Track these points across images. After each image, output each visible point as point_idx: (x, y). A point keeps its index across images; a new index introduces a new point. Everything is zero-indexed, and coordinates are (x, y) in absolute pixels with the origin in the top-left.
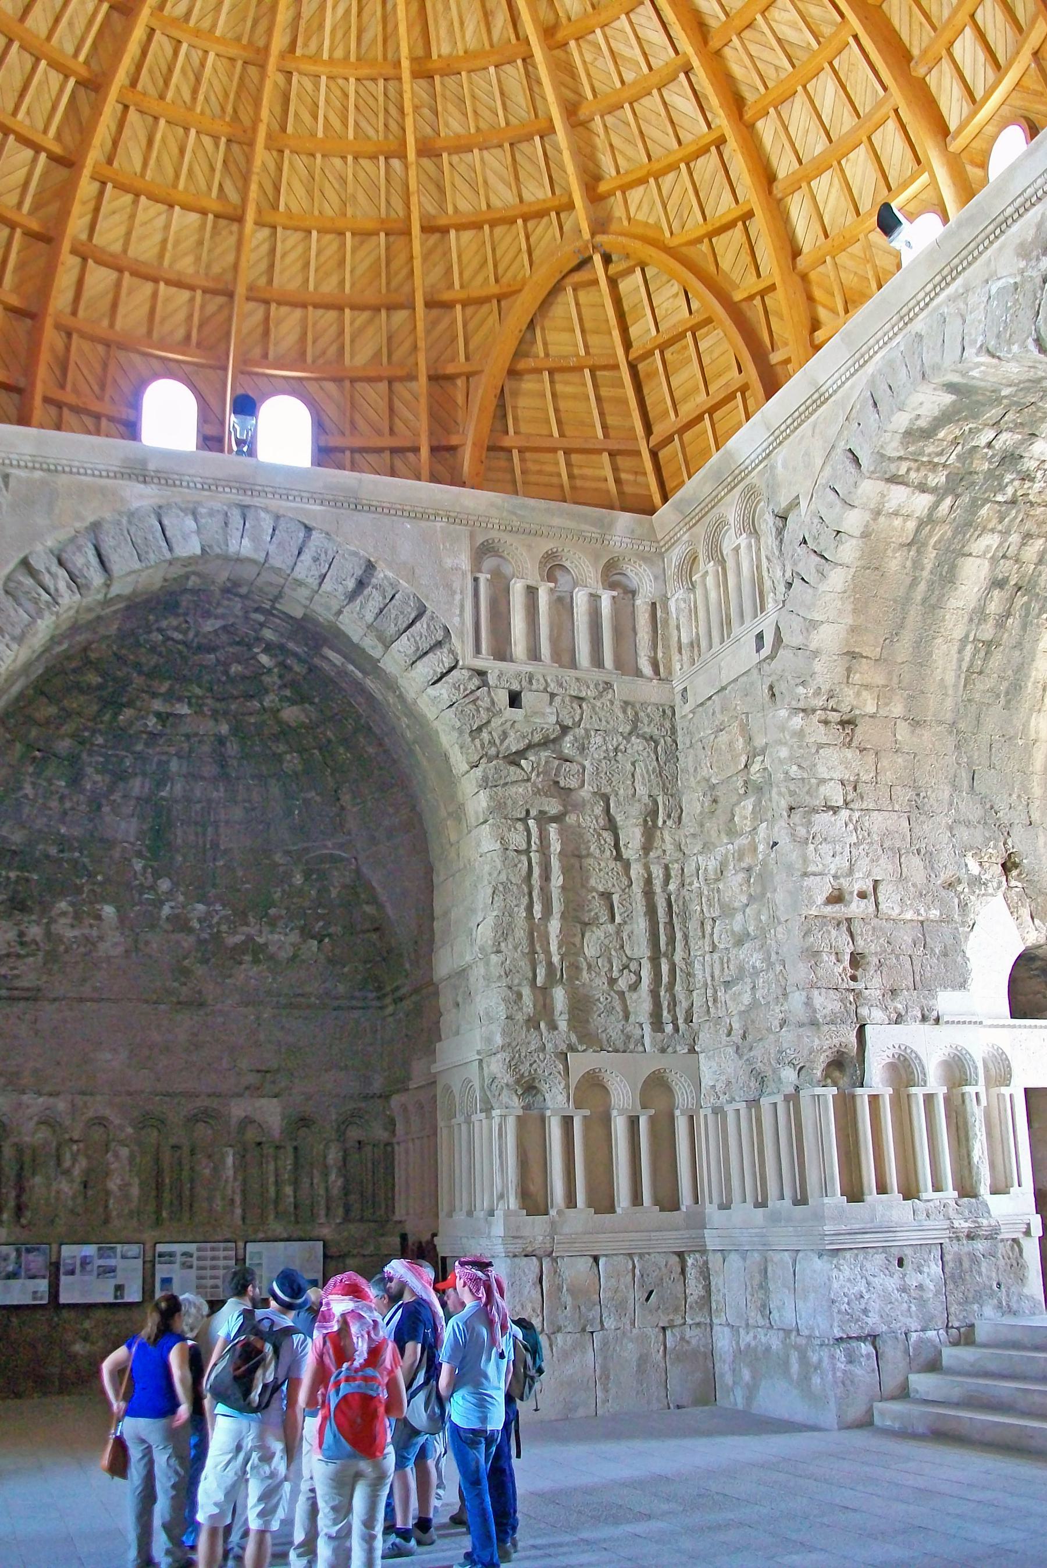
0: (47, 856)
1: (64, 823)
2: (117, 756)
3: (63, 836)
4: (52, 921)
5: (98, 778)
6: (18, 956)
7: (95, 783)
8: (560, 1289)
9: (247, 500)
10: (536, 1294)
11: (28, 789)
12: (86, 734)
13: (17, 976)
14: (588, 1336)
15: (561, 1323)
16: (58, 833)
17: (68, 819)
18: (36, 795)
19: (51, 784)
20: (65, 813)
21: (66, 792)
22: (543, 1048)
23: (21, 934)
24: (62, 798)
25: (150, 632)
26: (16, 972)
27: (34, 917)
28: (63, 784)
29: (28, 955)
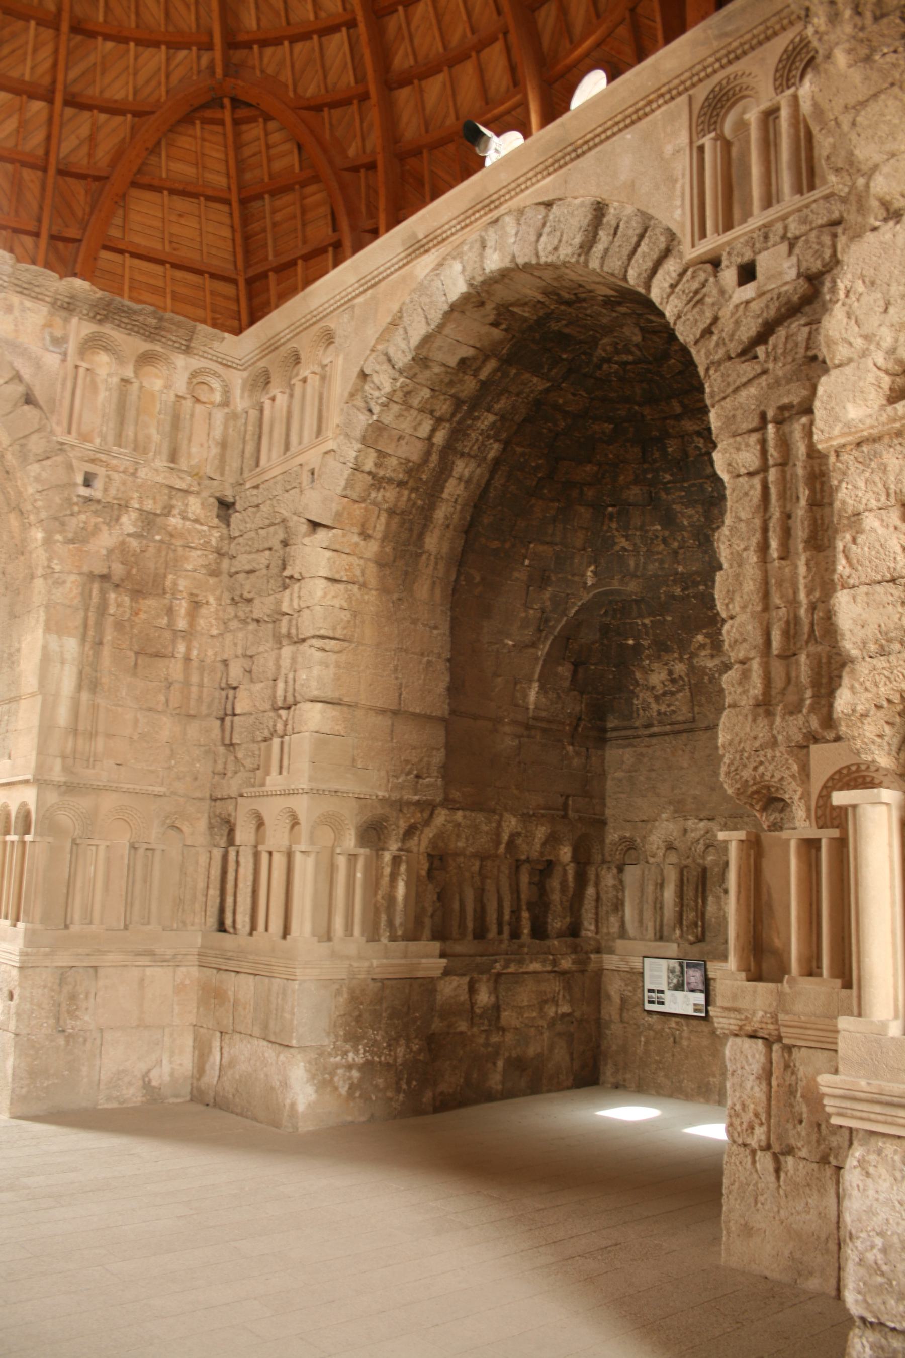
0: (673, 597)
1: (679, 564)
2: (694, 485)
3: (682, 574)
4: (693, 655)
5: (690, 511)
6: (673, 693)
7: (690, 517)
8: (792, 1092)
9: (495, 214)
10: (759, 1093)
11: (624, 543)
12: (649, 476)
13: (674, 712)
14: (829, 1172)
15: (792, 1141)
16: (677, 574)
17: (680, 557)
18: (635, 544)
19: (647, 531)
20: (676, 553)
21: (667, 533)
22: (774, 743)
23: (670, 673)
24: (664, 541)
25: (599, 367)
26: (673, 708)
27: (676, 655)
28: (659, 527)
29: (679, 691)
